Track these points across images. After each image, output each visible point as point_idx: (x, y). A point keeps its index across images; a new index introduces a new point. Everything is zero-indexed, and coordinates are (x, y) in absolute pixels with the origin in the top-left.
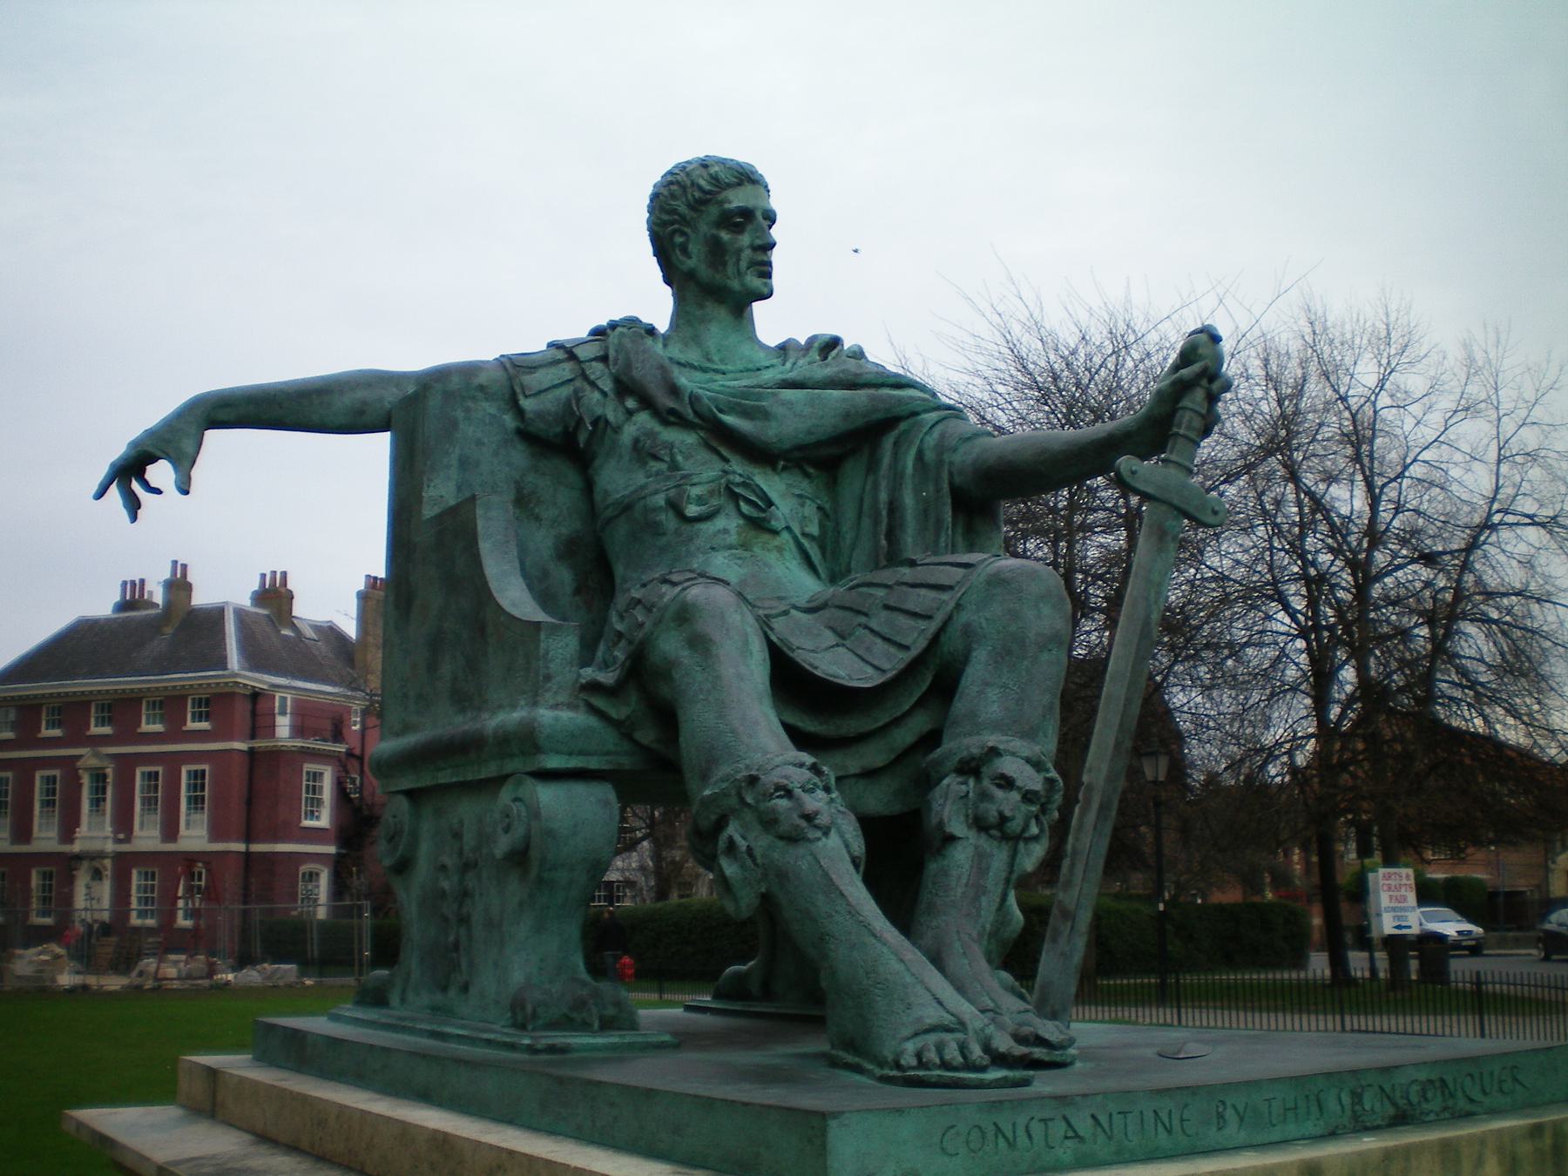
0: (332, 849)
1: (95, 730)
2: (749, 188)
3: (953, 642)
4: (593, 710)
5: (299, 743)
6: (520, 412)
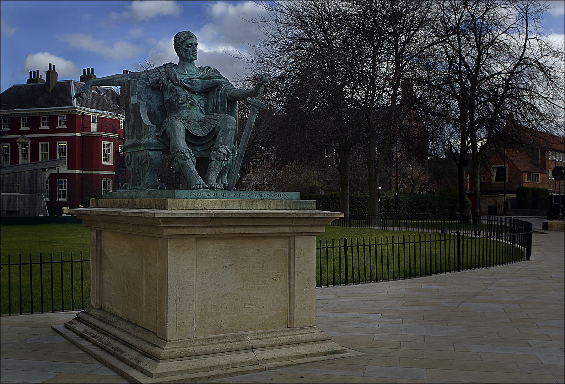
0: (114, 173)
1: (22, 128)
3: (217, 129)
4: (158, 139)
6: (149, 82)
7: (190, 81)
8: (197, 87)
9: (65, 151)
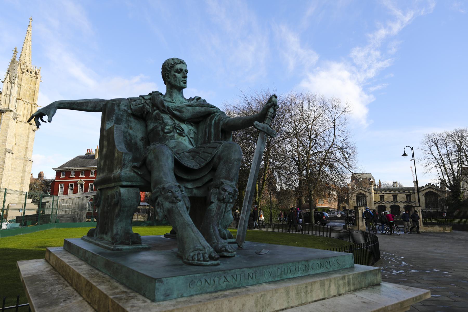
1: (81, 176)
2: (182, 64)
3: (215, 159)
4: (135, 172)
6: (131, 109)
7: (179, 109)
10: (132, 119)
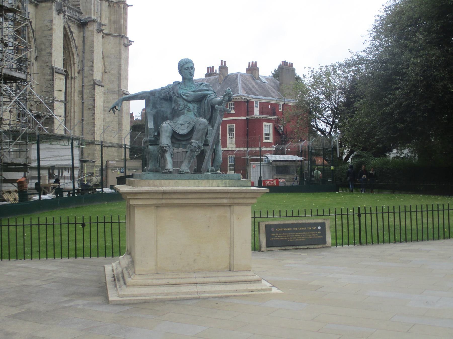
5: (262, 116)
8: (190, 99)
9: (233, 131)
10: (163, 101)
